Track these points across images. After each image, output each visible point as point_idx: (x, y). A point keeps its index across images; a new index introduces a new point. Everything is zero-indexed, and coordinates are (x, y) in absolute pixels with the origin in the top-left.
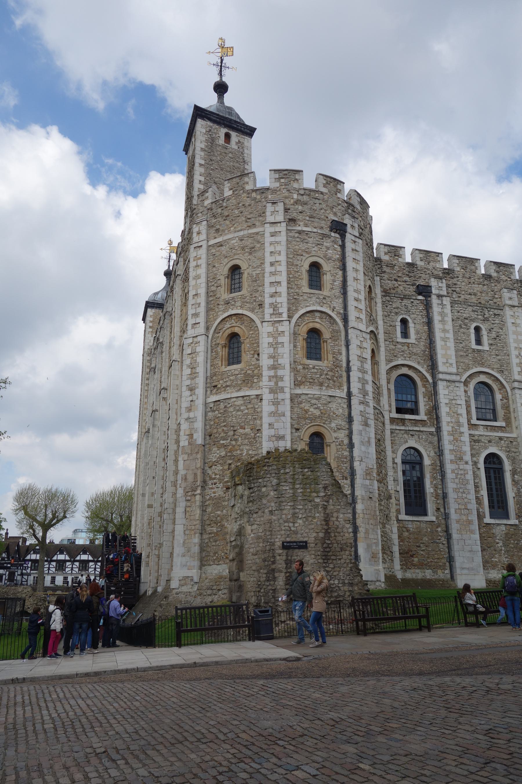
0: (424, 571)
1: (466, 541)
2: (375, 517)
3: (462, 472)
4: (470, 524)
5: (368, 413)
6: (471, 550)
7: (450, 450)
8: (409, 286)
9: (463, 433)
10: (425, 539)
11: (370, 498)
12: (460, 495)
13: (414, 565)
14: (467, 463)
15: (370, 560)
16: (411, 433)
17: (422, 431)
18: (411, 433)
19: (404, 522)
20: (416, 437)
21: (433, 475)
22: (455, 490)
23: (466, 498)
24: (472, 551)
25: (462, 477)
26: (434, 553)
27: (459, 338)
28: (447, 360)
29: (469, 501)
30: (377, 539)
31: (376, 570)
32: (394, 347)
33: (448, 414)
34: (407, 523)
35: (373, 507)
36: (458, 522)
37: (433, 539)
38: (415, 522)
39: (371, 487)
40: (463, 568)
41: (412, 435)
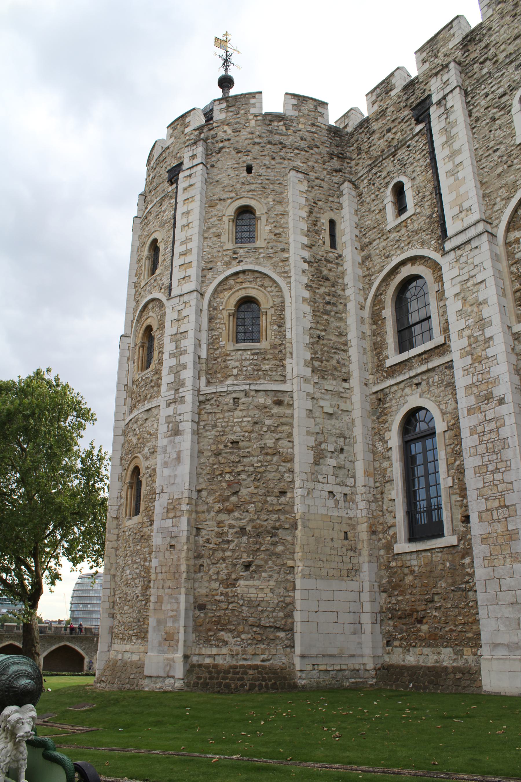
0: (438, 650)
1: (503, 581)
2: (177, 576)
3: (493, 425)
4: (511, 539)
5: (180, 415)
6: (513, 600)
7: (467, 387)
8: (409, 123)
9: (491, 338)
10: (442, 584)
11: (172, 546)
12: (489, 477)
13: (422, 639)
14: (501, 401)
15: (160, 644)
16: (415, 381)
17: (433, 369)
18: (415, 381)
19: (404, 557)
20: (424, 383)
21: (453, 449)
22: (479, 470)
23: (502, 481)
24: (517, 603)
25: (493, 436)
26: (455, 612)
27: (492, 144)
28: (461, 206)
29: (509, 486)
30: (177, 610)
31: (168, 659)
32: (384, 244)
33: (460, 313)
34: (408, 557)
35: (175, 560)
36: (484, 540)
37: (453, 584)
38: (424, 554)
39: (175, 529)
40: (496, 646)
41: (418, 385)
